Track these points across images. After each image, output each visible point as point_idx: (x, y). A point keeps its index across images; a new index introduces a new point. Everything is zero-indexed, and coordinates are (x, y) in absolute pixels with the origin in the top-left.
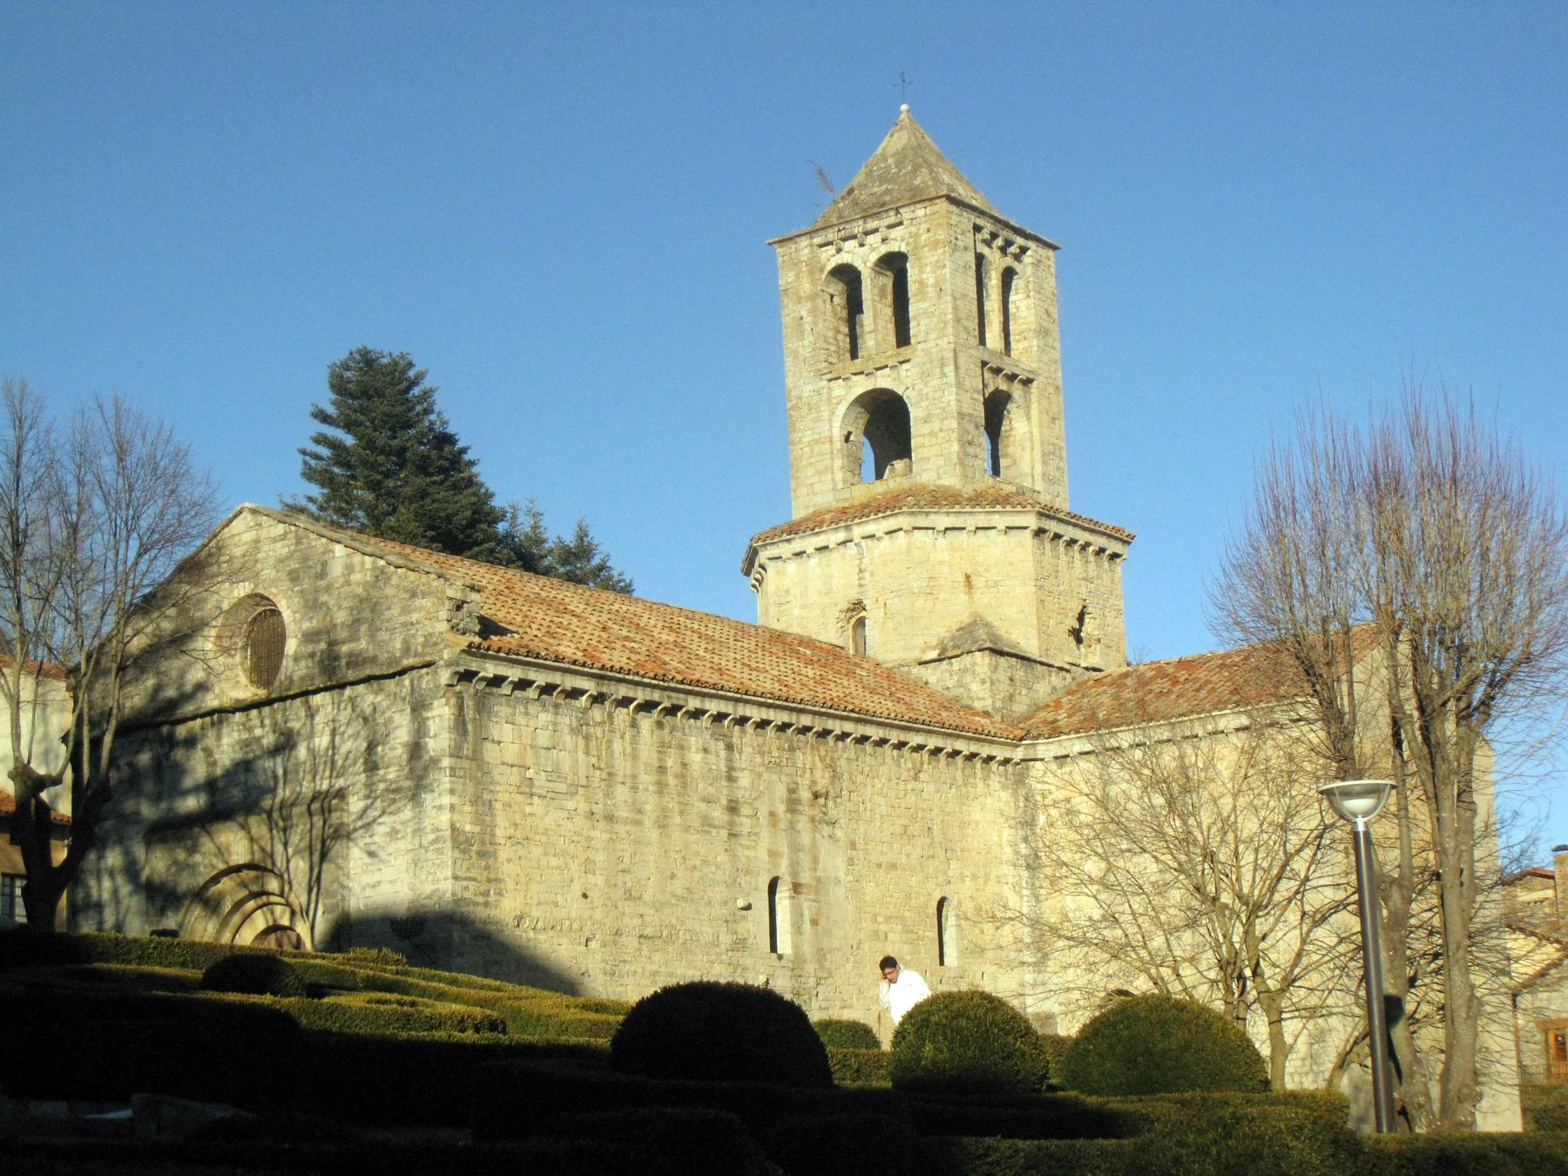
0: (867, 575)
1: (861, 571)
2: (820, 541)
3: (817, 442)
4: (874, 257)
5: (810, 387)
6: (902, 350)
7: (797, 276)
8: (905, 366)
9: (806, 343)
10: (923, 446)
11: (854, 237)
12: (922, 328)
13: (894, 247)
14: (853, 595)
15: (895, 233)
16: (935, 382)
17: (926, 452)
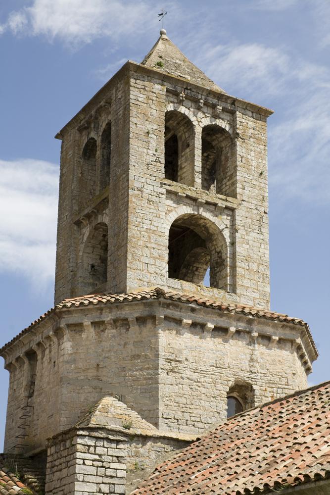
0: (257, 365)
1: (252, 360)
2: (223, 322)
3: (154, 231)
4: (206, 122)
5: (151, 188)
6: (229, 199)
7: (148, 98)
8: (226, 212)
9: (151, 152)
10: (243, 276)
11: (196, 101)
12: (246, 192)
13: (223, 124)
14: (244, 376)
15: (227, 116)
16: (253, 235)
17: (246, 283)
